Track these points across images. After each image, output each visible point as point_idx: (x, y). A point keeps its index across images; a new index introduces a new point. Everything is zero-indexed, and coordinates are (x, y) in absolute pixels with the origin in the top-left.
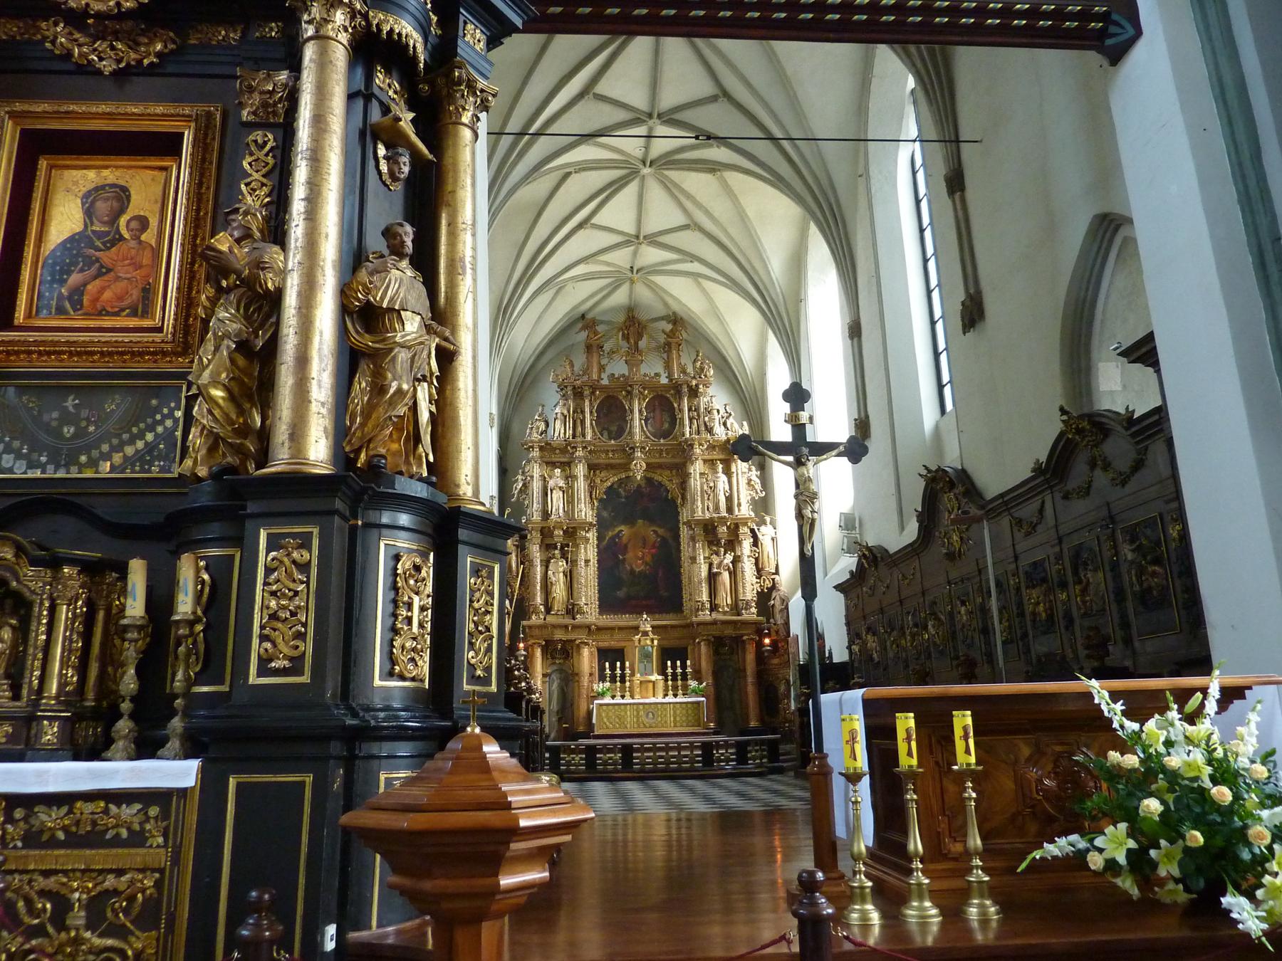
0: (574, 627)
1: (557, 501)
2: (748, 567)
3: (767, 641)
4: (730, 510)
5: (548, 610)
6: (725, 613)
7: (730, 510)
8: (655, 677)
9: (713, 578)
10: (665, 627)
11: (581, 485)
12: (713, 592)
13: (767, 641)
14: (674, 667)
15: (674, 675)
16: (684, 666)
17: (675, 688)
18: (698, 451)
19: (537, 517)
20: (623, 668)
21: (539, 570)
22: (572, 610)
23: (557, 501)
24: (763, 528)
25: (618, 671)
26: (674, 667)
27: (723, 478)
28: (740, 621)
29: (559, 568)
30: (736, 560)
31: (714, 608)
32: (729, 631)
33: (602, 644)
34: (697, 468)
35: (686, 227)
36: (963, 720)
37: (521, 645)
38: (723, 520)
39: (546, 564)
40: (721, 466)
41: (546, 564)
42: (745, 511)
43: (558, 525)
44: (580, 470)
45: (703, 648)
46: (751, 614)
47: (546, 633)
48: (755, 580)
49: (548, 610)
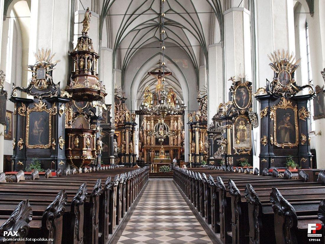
0: (151, 147)
1: (149, 127)
2: (179, 138)
3: (182, 150)
4: (177, 128)
5: (147, 144)
6: (175, 146)
7: (177, 128)
8: (164, 155)
9: (174, 140)
10: (166, 147)
11: (153, 124)
12: (174, 142)
13: (182, 150)
14: (166, 154)
15: (166, 155)
16: (168, 154)
17: (166, 157)
18: (172, 118)
19: (145, 129)
20: (158, 154)
21: (145, 138)
22: (151, 144)
23: (149, 127)
24: (183, 132)
25: (158, 154)
26: (166, 154)
27: (176, 123)
28: (178, 147)
29: (148, 138)
30: (178, 137)
31: (174, 145)
32: (176, 148)
33: (156, 150)
34: (172, 121)
35: (168, 85)
36: (156, 165)
37: (143, 150)
38: (175, 130)
39: (147, 137)
40: (176, 121)
41: (147, 137)
42: (179, 128)
43: (149, 131)
44: (152, 121)
45: (171, 151)
46: (179, 146)
47: (147, 148)
48: (181, 140)
49: (147, 144)
